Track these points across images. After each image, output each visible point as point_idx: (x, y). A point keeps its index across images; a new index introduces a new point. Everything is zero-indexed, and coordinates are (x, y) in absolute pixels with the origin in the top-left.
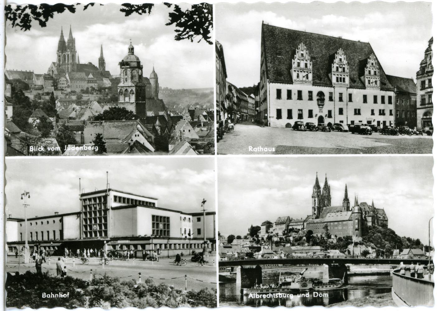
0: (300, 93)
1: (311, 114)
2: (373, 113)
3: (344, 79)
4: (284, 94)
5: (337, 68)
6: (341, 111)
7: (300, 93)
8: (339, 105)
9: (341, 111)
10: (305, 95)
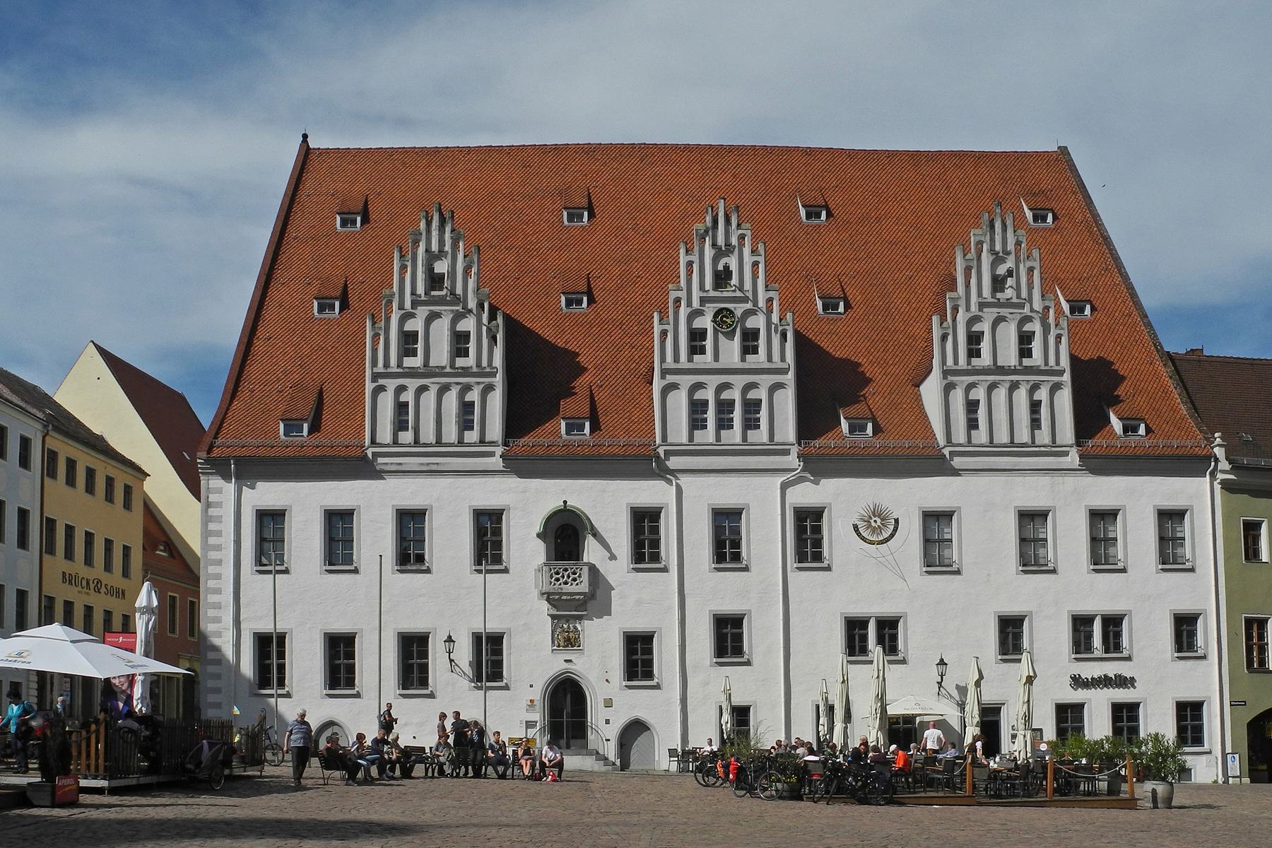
0: (410, 523)
1: (489, 659)
2: (1011, 632)
3: (752, 407)
4: (305, 538)
5: (697, 337)
6: (729, 637)
7: (410, 523)
8: (720, 592)
9: (729, 637)
10: (450, 540)
